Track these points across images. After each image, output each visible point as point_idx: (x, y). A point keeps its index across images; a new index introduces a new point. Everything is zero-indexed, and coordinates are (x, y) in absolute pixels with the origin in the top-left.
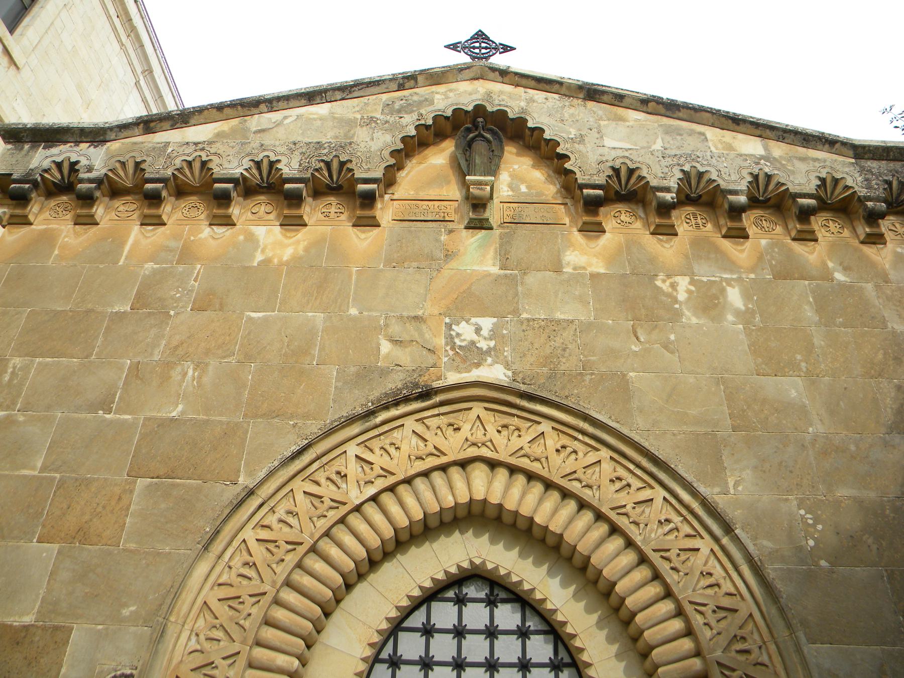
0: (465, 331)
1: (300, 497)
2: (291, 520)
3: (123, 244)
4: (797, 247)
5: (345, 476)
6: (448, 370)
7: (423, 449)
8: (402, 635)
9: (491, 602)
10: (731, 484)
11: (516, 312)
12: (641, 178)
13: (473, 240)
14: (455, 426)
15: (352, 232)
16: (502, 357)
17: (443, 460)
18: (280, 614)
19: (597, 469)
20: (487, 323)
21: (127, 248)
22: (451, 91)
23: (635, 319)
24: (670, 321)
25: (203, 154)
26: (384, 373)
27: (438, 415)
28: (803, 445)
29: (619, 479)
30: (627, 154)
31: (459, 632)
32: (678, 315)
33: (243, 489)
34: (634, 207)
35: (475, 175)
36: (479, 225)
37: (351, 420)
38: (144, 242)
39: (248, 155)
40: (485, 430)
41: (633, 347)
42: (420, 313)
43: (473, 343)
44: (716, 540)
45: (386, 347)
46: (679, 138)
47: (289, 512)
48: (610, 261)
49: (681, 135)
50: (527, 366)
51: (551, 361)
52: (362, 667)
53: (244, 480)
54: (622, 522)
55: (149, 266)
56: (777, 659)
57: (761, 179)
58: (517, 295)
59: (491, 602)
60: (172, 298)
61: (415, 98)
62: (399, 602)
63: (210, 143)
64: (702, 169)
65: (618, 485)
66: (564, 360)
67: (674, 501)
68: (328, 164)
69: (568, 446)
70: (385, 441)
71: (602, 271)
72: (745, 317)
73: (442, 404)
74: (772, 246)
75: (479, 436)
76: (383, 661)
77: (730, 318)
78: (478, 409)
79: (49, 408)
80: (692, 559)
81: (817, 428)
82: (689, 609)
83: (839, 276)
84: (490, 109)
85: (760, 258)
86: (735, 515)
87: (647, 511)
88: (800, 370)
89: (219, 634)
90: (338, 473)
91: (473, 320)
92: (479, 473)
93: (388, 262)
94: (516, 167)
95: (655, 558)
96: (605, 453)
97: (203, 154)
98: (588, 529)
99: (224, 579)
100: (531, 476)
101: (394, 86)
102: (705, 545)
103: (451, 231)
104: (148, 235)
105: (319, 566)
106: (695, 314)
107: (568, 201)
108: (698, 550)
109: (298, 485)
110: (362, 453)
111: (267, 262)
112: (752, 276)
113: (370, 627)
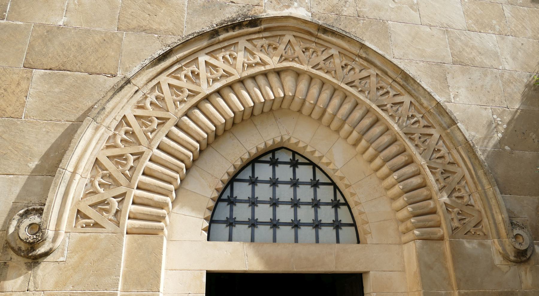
5: (198, 74)
6: (268, 9)
8: (236, 185)
9: (294, 164)
14: (274, 46)
16: (304, 4)
17: (268, 67)
19: (368, 81)
27: (262, 38)
28: (496, 77)
29: (382, 88)
31: (274, 183)
33: (122, 79)
40: (294, 50)
41: (390, 5)
44: (445, 129)
51: (337, 9)
52: (212, 204)
59: (294, 164)
62: (236, 162)
65: (381, 92)
66: (345, 9)
67: (417, 104)
69: (349, 65)
73: (266, 30)
76: (224, 200)
80: (428, 141)
87: (400, 109)
88: (494, 30)
90: (193, 72)
96: (373, 71)
108: (432, 135)
110: (210, 60)
113: (216, 178)
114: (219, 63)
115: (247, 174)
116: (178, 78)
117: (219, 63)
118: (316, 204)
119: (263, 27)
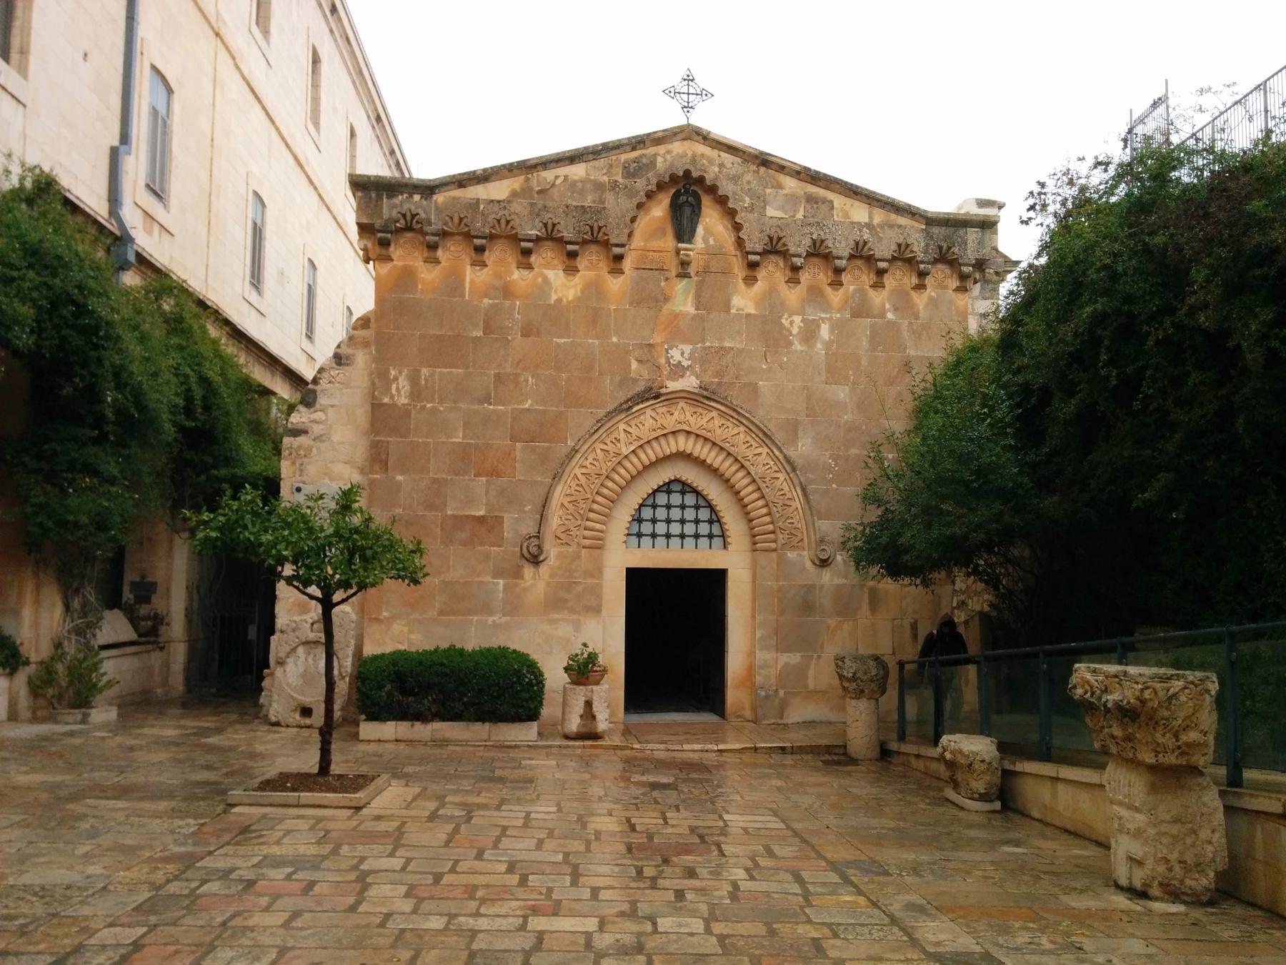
0: (676, 355)
1: (598, 451)
2: (595, 463)
3: (463, 280)
4: (871, 293)
7: (655, 426)
9: (683, 493)
10: (800, 445)
11: (703, 341)
12: (784, 245)
13: (680, 286)
15: (609, 278)
17: (665, 432)
18: (595, 507)
20: (687, 348)
21: (467, 285)
22: (668, 152)
23: (767, 346)
24: (786, 348)
25: (506, 212)
26: (635, 381)
30: (779, 223)
31: (668, 507)
32: (790, 343)
34: (778, 258)
35: (683, 242)
37: (621, 412)
38: (478, 280)
39: (538, 215)
42: (651, 341)
43: (680, 362)
45: (634, 365)
46: (815, 206)
47: (594, 459)
48: (758, 304)
49: (816, 203)
50: (707, 379)
54: (747, 464)
55: (486, 301)
56: (804, 527)
57: (861, 244)
58: (704, 329)
59: (683, 493)
60: (508, 327)
61: (644, 161)
63: (509, 202)
64: (823, 238)
65: (747, 445)
68: (592, 228)
70: (637, 421)
71: (753, 311)
72: (828, 345)
74: (856, 291)
77: (819, 346)
78: (682, 404)
79: (455, 402)
82: (771, 505)
83: (890, 316)
84: (695, 174)
85: (846, 302)
86: (799, 462)
89: (570, 517)
91: (681, 346)
93: (631, 303)
94: (707, 220)
96: (742, 429)
97: (506, 212)
98: (730, 466)
99: (568, 492)
100: (706, 439)
101: (629, 148)
102: (782, 476)
103: (667, 279)
104: (478, 274)
105: (610, 484)
106: (800, 344)
107: (738, 253)
109: (599, 446)
111: (559, 301)
112: (838, 315)
115: (650, 502)
118: (697, 522)
119: (663, 398)
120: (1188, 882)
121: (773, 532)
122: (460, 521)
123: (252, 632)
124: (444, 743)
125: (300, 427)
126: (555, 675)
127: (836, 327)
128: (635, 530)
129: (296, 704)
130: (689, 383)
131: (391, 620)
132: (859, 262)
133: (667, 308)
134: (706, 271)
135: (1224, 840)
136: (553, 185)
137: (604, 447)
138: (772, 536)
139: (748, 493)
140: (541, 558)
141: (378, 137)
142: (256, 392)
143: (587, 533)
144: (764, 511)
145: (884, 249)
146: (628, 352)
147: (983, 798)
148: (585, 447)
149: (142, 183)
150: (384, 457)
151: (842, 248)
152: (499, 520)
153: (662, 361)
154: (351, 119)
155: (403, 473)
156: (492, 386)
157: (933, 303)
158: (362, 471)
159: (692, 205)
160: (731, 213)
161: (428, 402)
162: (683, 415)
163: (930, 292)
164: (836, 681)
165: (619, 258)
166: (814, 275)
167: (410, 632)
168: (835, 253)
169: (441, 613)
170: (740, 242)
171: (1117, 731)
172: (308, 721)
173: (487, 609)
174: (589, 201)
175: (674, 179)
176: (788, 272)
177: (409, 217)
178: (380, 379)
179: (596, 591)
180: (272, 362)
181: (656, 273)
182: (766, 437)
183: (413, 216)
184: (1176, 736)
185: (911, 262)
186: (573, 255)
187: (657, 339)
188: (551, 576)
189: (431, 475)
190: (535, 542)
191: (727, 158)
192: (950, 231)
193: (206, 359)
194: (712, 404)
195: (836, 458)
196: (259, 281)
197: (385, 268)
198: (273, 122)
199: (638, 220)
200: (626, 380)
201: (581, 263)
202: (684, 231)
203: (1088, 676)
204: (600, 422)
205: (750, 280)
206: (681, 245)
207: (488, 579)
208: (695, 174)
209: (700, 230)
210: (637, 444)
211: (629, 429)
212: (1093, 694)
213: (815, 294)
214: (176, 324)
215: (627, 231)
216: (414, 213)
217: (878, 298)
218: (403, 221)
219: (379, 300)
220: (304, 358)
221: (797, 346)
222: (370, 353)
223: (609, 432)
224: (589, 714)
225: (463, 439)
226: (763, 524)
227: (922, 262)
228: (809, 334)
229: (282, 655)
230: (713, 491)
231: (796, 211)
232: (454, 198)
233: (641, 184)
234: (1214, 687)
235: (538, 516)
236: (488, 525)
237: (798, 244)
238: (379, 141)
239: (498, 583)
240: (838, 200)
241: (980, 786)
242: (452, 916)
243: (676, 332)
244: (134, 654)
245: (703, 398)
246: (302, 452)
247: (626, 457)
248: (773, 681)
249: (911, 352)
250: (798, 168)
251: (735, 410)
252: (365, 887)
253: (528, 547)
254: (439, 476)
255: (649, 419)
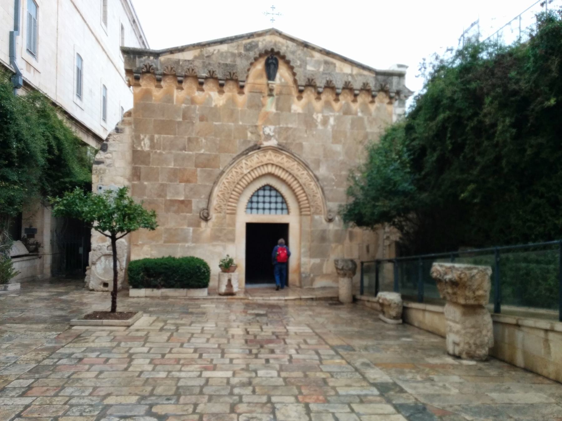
1: (234, 172)
2: (232, 177)
11: (279, 124)
17: (263, 164)
18: (232, 196)
20: (272, 127)
26: (249, 142)
32: (316, 126)
36: (271, 95)
45: (249, 134)
53: (221, 169)
54: (298, 178)
61: (253, 44)
68: (230, 73)
70: (250, 159)
72: (333, 127)
75: (270, 158)
78: (270, 152)
81: (341, 158)
83: (360, 114)
86: (320, 177)
89: (221, 201)
92: (270, 167)
93: (248, 107)
95: (303, 185)
96: (296, 163)
99: (221, 190)
102: (313, 183)
107: (295, 86)
109: (234, 170)
111: (216, 106)
114: (249, 163)
116: (237, 169)
117: (249, 163)
120: (478, 352)
121: (309, 207)
122: (173, 202)
123: (81, 250)
124: (166, 297)
125: (101, 160)
126: (215, 268)
127: (337, 119)
128: (250, 205)
129: (101, 281)
130: (273, 143)
131: (143, 245)
132: (347, 91)
133: (264, 110)
134: (280, 94)
135: (492, 335)
136: (213, 54)
137: (236, 170)
138: (308, 209)
139: (298, 191)
140: (209, 218)
141: (134, 30)
142: (80, 144)
143: (229, 208)
144: (305, 198)
145: (357, 85)
146: (246, 129)
147: (395, 318)
148: (228, 170)
149: (25, 48)
150: (138, 174)
151: (339, 84)
152: (190, 202)
153: (261, 133)
154: (121, 21)
155: (148, 180)
156: (186, 143)
157: (378, 109)
158: (129, 180)
159: (274, 64)
160: (291, 68)
161: (158, 149)
162: (270, 157)
163: (377, 104)
164: (335, 270)
165: (242, 87)
166: (327, 96)
167: (151, 250)
168: (336, 86)
169: (165, 242)
170: (295, 81)
171: (450, 290)
172: (106, 289)
173: (185, 240)
174: (229, 61)
175: (266, 52)
176: (316, 94)
177: (148, 67)
178: (136, 139)
179: (233, 232)
180: (88, 131)
181: (259, 94)
182: (306, 166)
183: (150, 66)
184: (474, 292)
185: (369, 91)
186: (222, 85)
187: (259, 123)
188: (214, 226)
189: (160, 182)
190: (206, 211)
191: (290, 43)
192: (386, 77)
193: (57, 129)
194: (283, 152)
195: (336, 176)
196: (80, 95)
197: (138, 90)
198: (85, 22)
199: (251, 71)
200: (246, 141)
201: (226, 89)
202: (271, 76)
203: (439, 268)
204: (235, 159)
205: (300, 98)
206: (270, 82)
207: (185, 227)
208: (276, 50)
209: (278, 75)
210: (250, 169)
211: (247, 163)
212: (440, 276)
213: (328, 104)
214: (43, 114)
215: (246, 75)
216: (150, 65)
217: (355, 107)
218: (145, 69)
219: (136, 104)
220: (102, 129)
221: (320, 127)
222: (132, 128)
223: (238, 164)
224: (230, 285)
225: (174, 166)
226: (305, 203)
227: (374, 91)
228: (325, 122)
229: (94, 260)
230: (283, 190)
231: (319, 68)
232: (169, 59)
233: (252, 54)
234: (490, 272)
235: (207, 200)
236: (185, 204)
237: (321, 83)
238: (135, 32)
239: (190, 229)
240: (338, 63)
241: (393, 313)
242: (169, 372)
243: (267, 121)
244: (27, 260)
245: (279, 149)
246: (102, 172)
247: (246, 175)
248: (308, 270)
249: (369, 130)
250: (321, 49)
251: (293, 155)
252: (132, 360)
253: (203, 214)
254: (164, 182)
255: (256, 158)
